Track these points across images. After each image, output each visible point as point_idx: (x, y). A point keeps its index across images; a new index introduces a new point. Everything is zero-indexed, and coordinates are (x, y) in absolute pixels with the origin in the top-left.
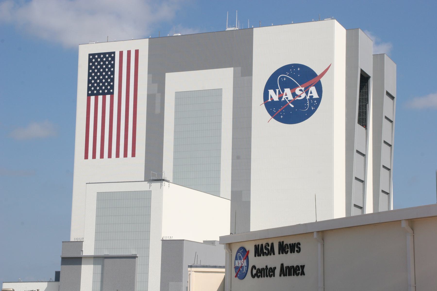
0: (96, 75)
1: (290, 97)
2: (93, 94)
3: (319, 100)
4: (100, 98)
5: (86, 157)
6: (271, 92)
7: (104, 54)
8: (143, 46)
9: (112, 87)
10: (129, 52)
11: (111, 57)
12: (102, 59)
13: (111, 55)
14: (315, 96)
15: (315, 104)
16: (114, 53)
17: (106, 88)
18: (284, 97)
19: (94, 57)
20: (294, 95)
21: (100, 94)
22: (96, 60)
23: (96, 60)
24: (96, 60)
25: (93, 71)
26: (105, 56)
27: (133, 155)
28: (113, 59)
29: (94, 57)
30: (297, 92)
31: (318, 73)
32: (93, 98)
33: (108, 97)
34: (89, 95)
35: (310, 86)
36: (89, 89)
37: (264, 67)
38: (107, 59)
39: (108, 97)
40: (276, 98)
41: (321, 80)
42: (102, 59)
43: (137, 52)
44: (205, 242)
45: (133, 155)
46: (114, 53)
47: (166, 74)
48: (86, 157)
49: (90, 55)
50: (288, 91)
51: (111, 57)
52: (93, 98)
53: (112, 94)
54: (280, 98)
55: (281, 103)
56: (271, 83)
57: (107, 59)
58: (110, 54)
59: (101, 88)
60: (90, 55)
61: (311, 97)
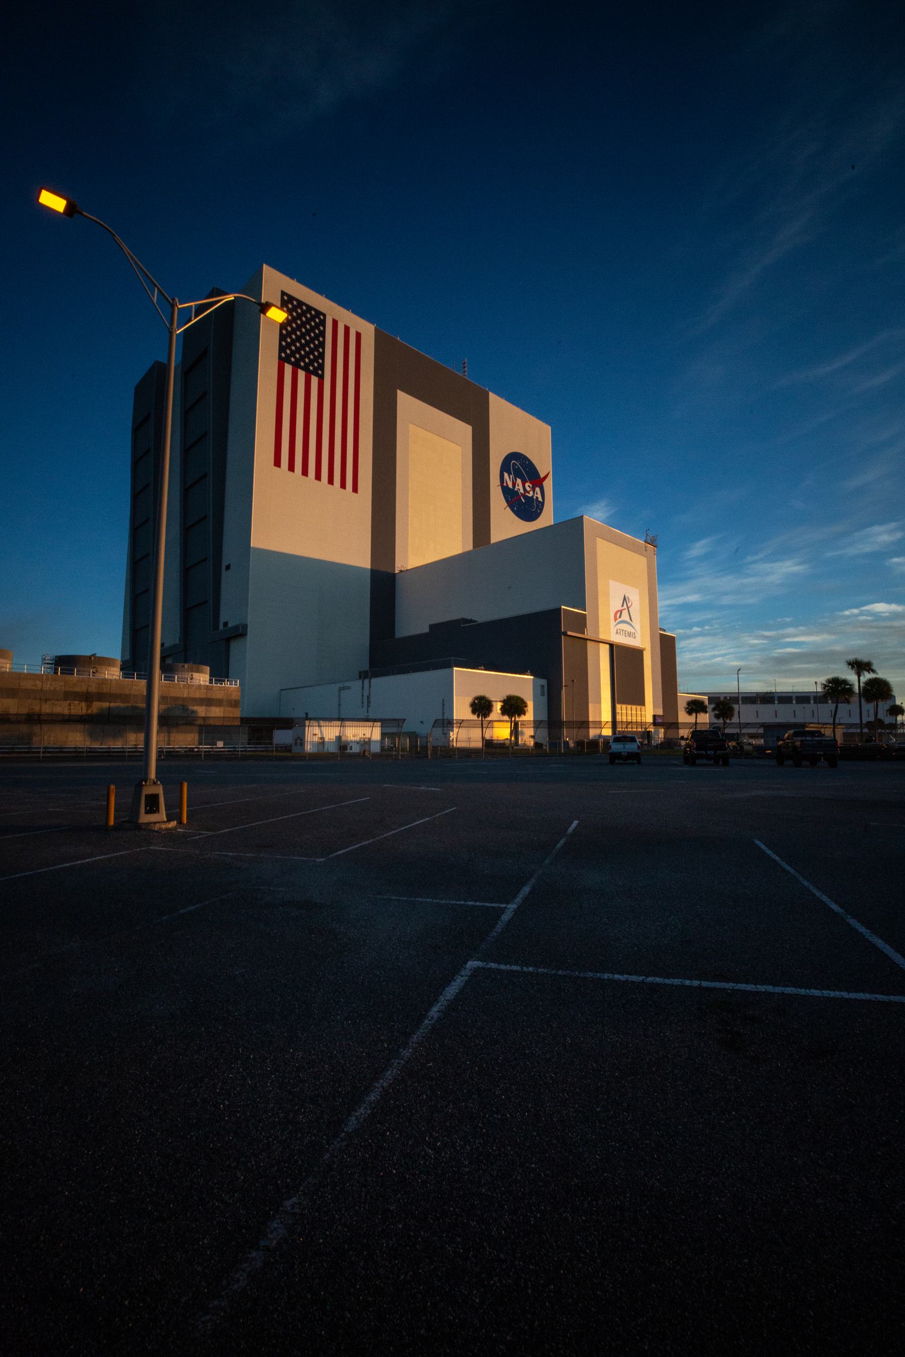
1: (522, 491)
3: (543, 504)
4: (301, 375)
5: (277, 463)
6: (506, 475)
7: (308, 307)
9: (321, 366)
10: (347, 329)
11: (319, 318)
21: (302, 368)
27: (355, 489)
28: (323, 323)
31: (542, 476)
32: (288, 369)
33: (314, 380)
34: (282, 361)
36: (282, 349)
39: (314, 380)
40: (510, 486)
43: (358, 335)
45: (355, 489)
46: (324, 315)
47: (399, 391)
48: (277, 463)
50: (519, 481)
51: (319, 318)
53: (321, 378)
56: (506, 466)
58: (319, 313)
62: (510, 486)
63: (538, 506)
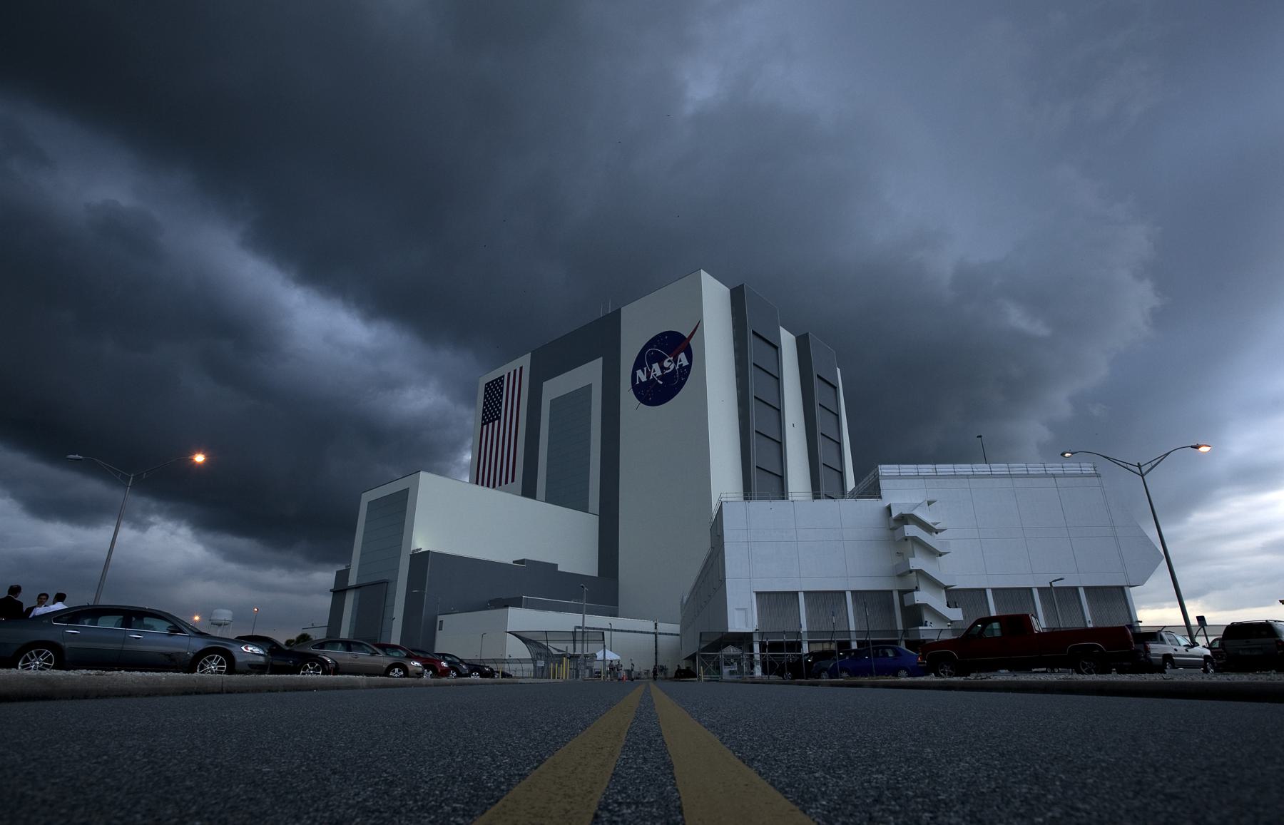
1: (659, 373)
3: (689, 367)
6: (639, 372)
8: (525, 361)
14: (685, 363)
20: (662, 368)
30: (666, 364)
37: (632, 344)
40: (644, 379)
41: (691, 342)
50: (656, 366)
53: (499, 418)
54: (648, 377)
55: (651, 382)
62: (644, 379)
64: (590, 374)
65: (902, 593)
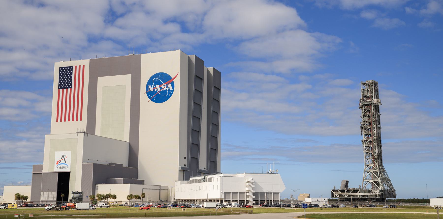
0: (63, 78)
1: (159, 90)
2: (61, 88)
3: (173, 91)
5: (57, 121)
6: (150, 87)
7: (67, 67)
8: (86, 62)
9: (71, 84)
10: (80, 66)
12: (66, 70)
13: (71, 68)
14: (171, 89)
15: (171, 93)
16: (72, 67)
17: (68, 85)
18: (156, 89)
19: (62, 69)
20: (161, 88)
22: (63, 70)
23: (63, 71)
24: (63, 71)
25: (62, 76)
26: (67, 69)
27: (81, 119)
28: (72, 70)
29: (62, 69)
30: (162, 87)
34: (59, 89)
35: (169, 84)
36: (59, 85)
38: (69, 70)
40: (152, 90)
41: (174, 81)
42: (66, 70)
43: (84, 66)
44: (109, 164)
45: (81, 119)
46: (72, 67)
48: (57, 121)
49: (60, 68)
50: (158, 86)
52: (61, 90)
53: (71, 88)
54: (154, 90)
55: (154, 92)
56: (150, 83)
57: (69, 70)
58: (70, 67)
59: (65, 85)
60: (60, 68)
61: (169, 89)
63: (169, 93)
64: (126, 80)
65: (246, 193)
